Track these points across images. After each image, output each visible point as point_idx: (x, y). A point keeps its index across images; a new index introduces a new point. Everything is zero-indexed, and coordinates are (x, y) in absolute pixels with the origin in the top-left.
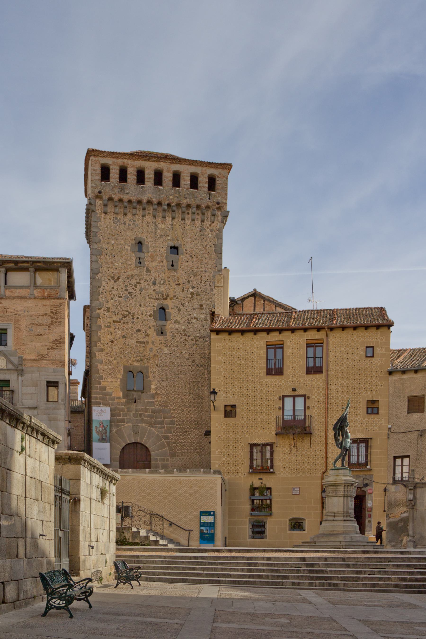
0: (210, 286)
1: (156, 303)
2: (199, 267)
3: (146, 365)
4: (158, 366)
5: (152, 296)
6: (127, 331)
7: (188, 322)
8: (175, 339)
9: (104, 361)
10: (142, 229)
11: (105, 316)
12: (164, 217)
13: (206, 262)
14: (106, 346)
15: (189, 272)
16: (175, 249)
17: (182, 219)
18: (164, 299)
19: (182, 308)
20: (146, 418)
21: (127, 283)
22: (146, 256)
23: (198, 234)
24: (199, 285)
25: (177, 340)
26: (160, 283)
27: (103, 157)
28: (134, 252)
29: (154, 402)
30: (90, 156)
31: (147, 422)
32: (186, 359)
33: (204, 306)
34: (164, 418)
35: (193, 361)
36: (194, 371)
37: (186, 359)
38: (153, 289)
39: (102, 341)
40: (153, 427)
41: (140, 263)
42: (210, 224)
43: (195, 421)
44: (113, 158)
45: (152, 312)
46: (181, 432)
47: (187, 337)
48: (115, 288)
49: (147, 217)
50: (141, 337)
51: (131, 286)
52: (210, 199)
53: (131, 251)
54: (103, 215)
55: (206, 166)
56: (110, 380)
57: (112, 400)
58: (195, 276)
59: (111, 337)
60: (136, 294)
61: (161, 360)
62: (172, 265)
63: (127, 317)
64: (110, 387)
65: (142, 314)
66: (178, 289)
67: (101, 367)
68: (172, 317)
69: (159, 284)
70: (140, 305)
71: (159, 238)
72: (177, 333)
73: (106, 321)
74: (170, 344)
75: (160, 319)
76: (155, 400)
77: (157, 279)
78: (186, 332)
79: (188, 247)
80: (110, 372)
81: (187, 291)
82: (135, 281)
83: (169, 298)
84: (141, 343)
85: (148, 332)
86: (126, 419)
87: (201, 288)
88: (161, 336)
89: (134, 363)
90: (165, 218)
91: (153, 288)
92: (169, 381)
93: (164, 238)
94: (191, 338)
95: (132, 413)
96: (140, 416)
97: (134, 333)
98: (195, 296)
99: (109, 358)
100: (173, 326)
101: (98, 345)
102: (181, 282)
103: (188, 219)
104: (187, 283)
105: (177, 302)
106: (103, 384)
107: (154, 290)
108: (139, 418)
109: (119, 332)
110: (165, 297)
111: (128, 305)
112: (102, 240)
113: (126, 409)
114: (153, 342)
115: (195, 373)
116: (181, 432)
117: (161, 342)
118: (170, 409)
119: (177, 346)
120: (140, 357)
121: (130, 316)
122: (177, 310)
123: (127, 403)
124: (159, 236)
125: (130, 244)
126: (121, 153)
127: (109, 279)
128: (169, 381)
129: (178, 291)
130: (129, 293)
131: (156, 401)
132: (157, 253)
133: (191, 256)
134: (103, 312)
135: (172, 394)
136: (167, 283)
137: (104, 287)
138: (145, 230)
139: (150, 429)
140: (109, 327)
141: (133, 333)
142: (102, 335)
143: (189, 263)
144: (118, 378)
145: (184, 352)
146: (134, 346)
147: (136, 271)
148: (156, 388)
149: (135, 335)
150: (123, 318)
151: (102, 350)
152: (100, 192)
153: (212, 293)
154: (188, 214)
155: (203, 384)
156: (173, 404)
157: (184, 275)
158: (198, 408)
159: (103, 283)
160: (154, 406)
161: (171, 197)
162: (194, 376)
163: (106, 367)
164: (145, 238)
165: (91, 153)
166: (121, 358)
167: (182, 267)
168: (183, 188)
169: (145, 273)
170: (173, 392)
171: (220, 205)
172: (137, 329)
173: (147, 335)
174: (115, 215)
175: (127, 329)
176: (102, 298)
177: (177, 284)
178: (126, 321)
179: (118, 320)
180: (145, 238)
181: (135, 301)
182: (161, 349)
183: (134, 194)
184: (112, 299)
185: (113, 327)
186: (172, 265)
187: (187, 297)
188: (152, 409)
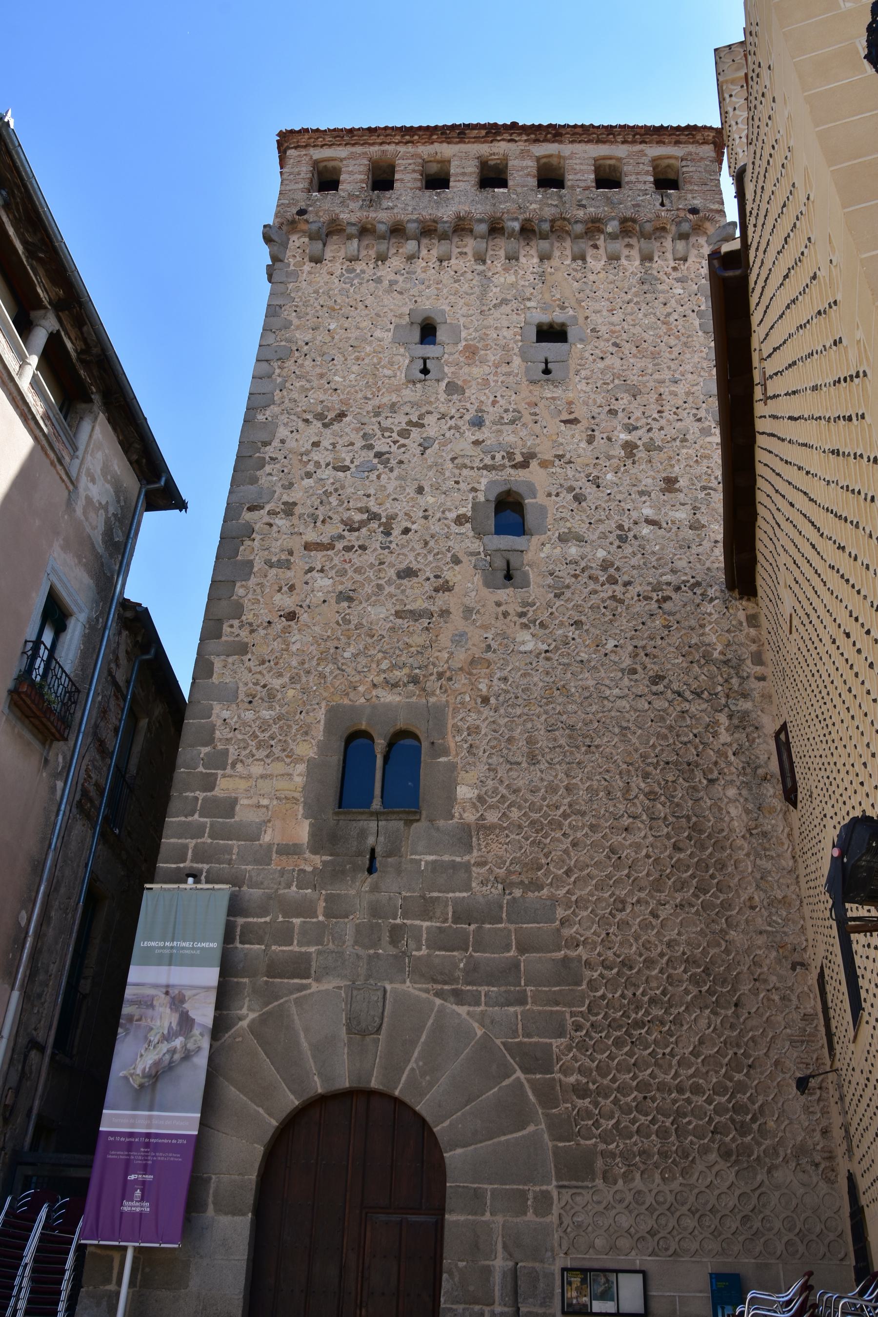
0: (699, 420)
1: (484, 480)
2: (650, 371)
3: (432, 700)
4: (493, 701)
5: (467, 461)
6: (357, 577)
7: (619, 537)
8: (568, 594)
9: (242, 689)
10: (438, 289)
11: (275, 528)
12: (512, 257)
13: (673, 357)
14: (262, 632)
15: (611, 386)
16: (552, 334)
17: (574, 259)
18: (514, 467)
19: (589, 490)
20: (424, 951)
21: (372, 427)
22: (446, 352)
23: (634, 290)
24: (654, 419)
25: (578, 599)
26: (500, 421)
27: (322, 146)
28: (405, 344)
29: (467, 867)
30: (285, 152)
31: (426, 973)
32: (622, 671)
33: (682, 483)
34: (522, 950)
35: (657, 679)
36: (663, 719)
37: (622, 671)
38: (474, 438)
39: (248, 617)
40: (459, 997)
41: (425, 371)
42: (672, 264)
43: (690, 961)
44: (353, 145)
45: (467, 510)
46: (613, 1025)
47: (619, 589)
48: (326, 443)
49: (453, 261)
50: (416, 594)
51: (387, 434)
52: (662, 204)
53: (393, 342)
54: (308, 267)
55: (643, 142)
56: (257, 769)
57: (257, 862)
58: (634, 396)
59: (287, 602)
60: (406, 456)
61: (505, 679)
62: (547, 371)
63: (364, 530)
64: (254, 801)
65: (426, 518)
66: (573, 436)
67: (226, 714)
68: (550, 520)
69: (494, 423)
70: (420, 490)
71: (495, 306)
72: (576, 576)
73: (276, 546)
74: (544, 616)
75: (500, 530)
76: (475, 853)
77: (491, 409)
78: (612, 571)
79: (600, 321)
80: (261, 736)
81: (609, 439)
82: (406, 419)
83: (534, 464)
84: (416, 615)
85: (448, 575)
86: (319, 953)
87: (661, 428)
88: (505, 587)
89: (379, 692)
90: (517, 259)
91: (471, 435)
92: (544, 766)
93: (514, 304)
94: (633, 591)
95: (349, 927)
96: (394, 940)
97: (389, 582)
98: (641, 454)
99: (268, 678)
100: (558, 551)
101: (226, 629)
102: (580, 412)
103: (595, 258)
104: (603, 416)
105: (570, 473)
106: (224, 787)
107: (476, 443)
108: (385, 950)
109: (323, 582)
110: (519, 458)
111: (372, 491)
112: (296, 322)
113: (322, 904)
114: (468, 611)
115: (671, 728)
116: (613, 1025)
117: (503, 608)
118: (554, 901)
119: (578, 624)
120: (406, 671)
121: (374, 525)
122: (570, 497)
123: (334, 873)
124: (495, 302)
125: (392, 327)
126: (376, 129)
127: (306, 421)
128: (544, 766)
129: (573, 441)
130: (379, 455)
131: (481, 864)
132: (489, 342)
133: (615, 345)
134: (267, 519)
135: (560, 826)
136: (527, 418)
137: (283, 442)
138: (445, 291)
139: (441, 1011)
140: (286, 565)
141: (380, 582)
142: (250, 596)
143: (608, 361)
144: (300, 760)
145: (611, 644)
146: (382, 628)
147: (408, 394)
148: (480, 798)
149: (388, 589)
150: (346, 533)
151: (242, 649)
152: (302, 212)
153: (709, 439)
154: (596, 247)
155: (715, 775)
156: (568, 873)
157: (593, 396)
158: (702, 889)
159: (282, 432)
160: (468, 888)
161: (534, 206)
162: (665, 737)
163: (249, 715)
164: (447, 308)
165: (286, 141)
166: (322, 676)
167: (583, 373)
168: (573, 188)
169: (443, 397)
170: (565, 816)
171: (701, 214)
172: (403, 566)
173: (446, 588)
174: (348, 263)
175: (358, 571)
176: (270, 474)
177: (565, 422)
178: (356, 544)
179: (326, 540)
180: (447, 308)
181: (398, 478)
182: (504, 635)
183: (410, 209)
184: (309, 475)
185: (299, 562)
186: (547, 371)
187: (609, 458)
188: (456, 901)
